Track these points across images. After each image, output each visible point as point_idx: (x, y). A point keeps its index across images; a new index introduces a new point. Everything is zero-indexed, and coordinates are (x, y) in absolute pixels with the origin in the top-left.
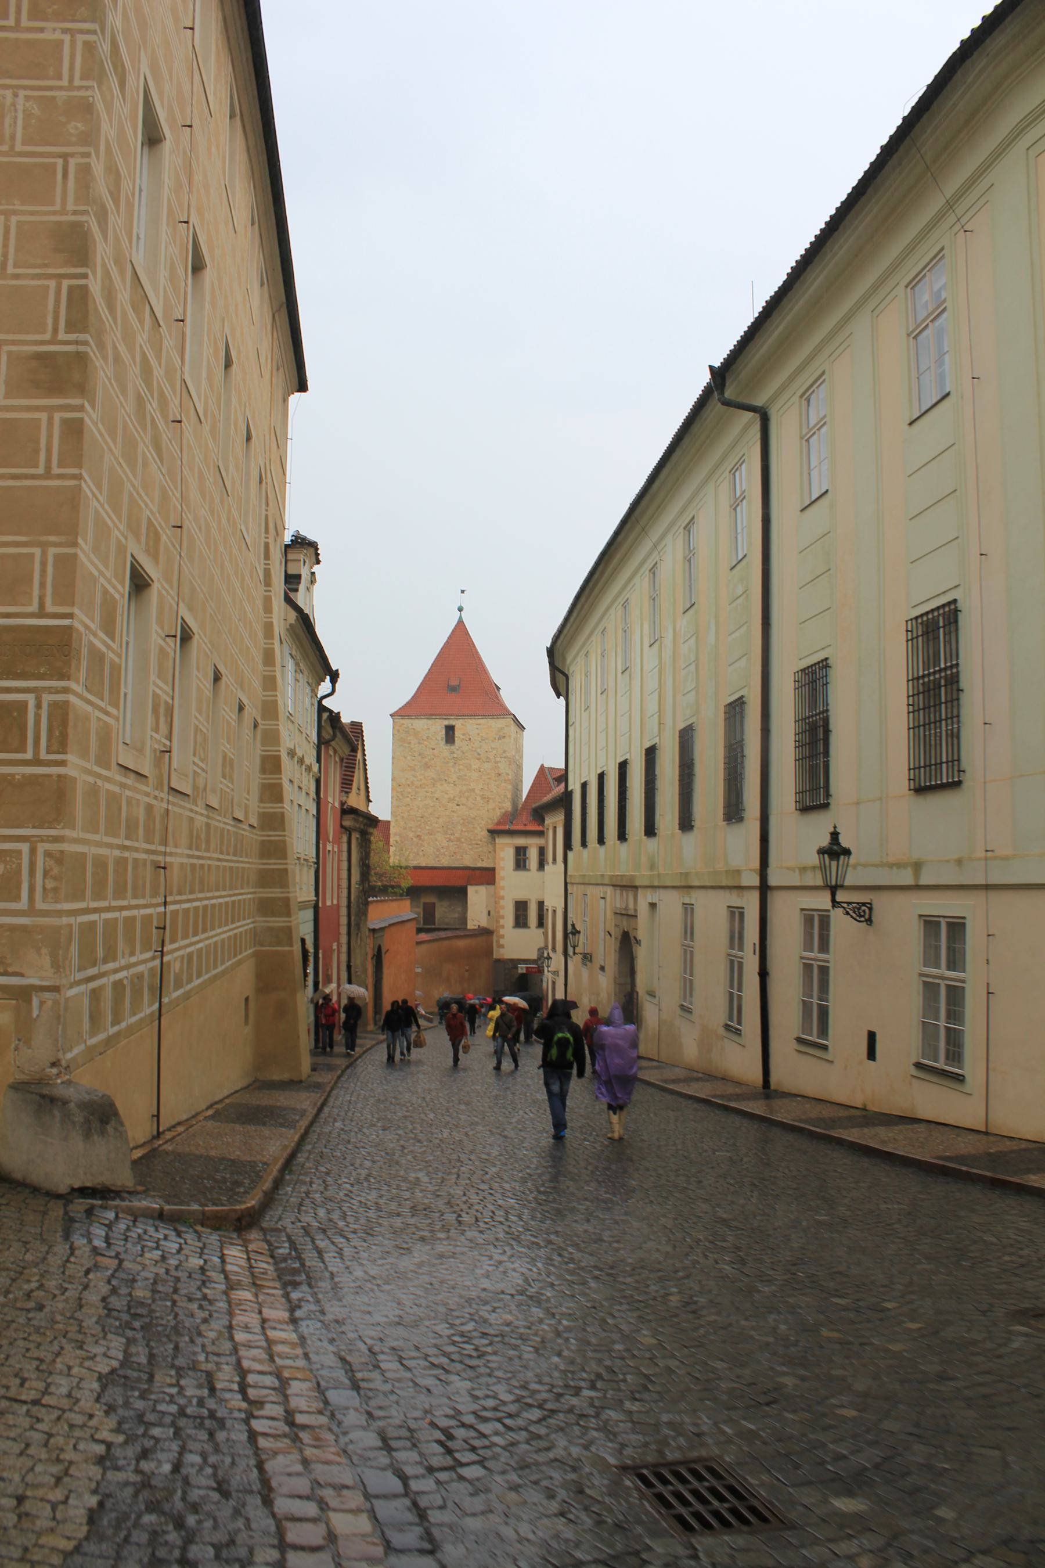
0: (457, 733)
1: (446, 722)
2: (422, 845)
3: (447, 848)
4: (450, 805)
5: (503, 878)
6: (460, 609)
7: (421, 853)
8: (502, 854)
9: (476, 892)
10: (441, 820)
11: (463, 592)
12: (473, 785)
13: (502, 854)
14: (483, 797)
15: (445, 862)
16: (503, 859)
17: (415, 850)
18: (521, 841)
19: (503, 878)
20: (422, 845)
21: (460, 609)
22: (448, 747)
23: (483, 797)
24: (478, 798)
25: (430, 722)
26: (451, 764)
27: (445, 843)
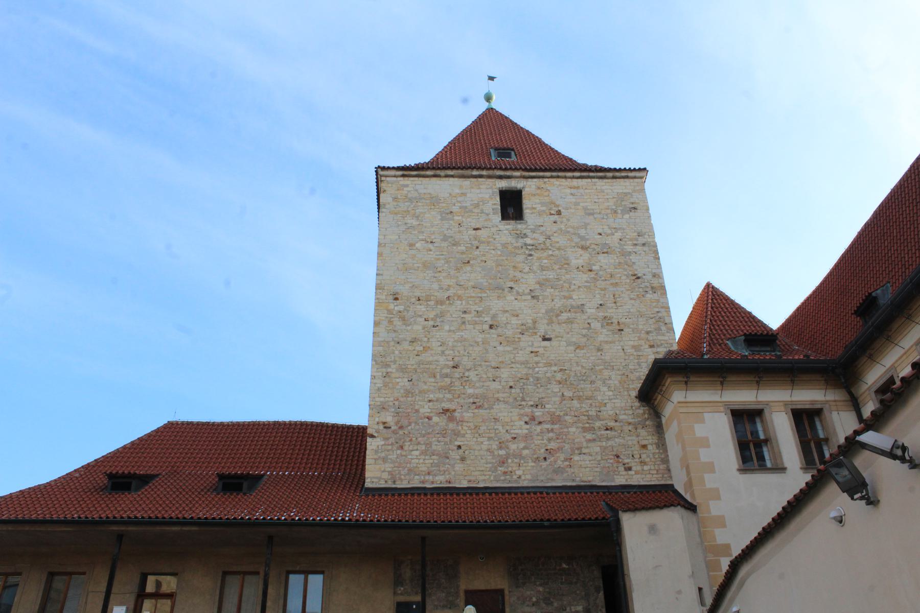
0: (527, 203)
1: (504, 184)
2: (457, 434)
3: (526, 437)
4: (524, 338)
5: (715, 495)
6: (488, 98)
7: (455, 455)
8: (700, 430)
9: (653, 529)
10: (505, 374)
11: (491, 78)
12: (578, 297)
13: (700, 430)
14: (607, 321)
15: (525, 475)
16: (704, 442)
17: (437, 447)
18: (744, 396)
19: (715, 495)
20: (457, 434)
21: (488, 98)
22: (510, 225)
23: (607, 321)
24: (596, 325)
25: (467, 182)
26: (521, 258)
27: (520, 428)
